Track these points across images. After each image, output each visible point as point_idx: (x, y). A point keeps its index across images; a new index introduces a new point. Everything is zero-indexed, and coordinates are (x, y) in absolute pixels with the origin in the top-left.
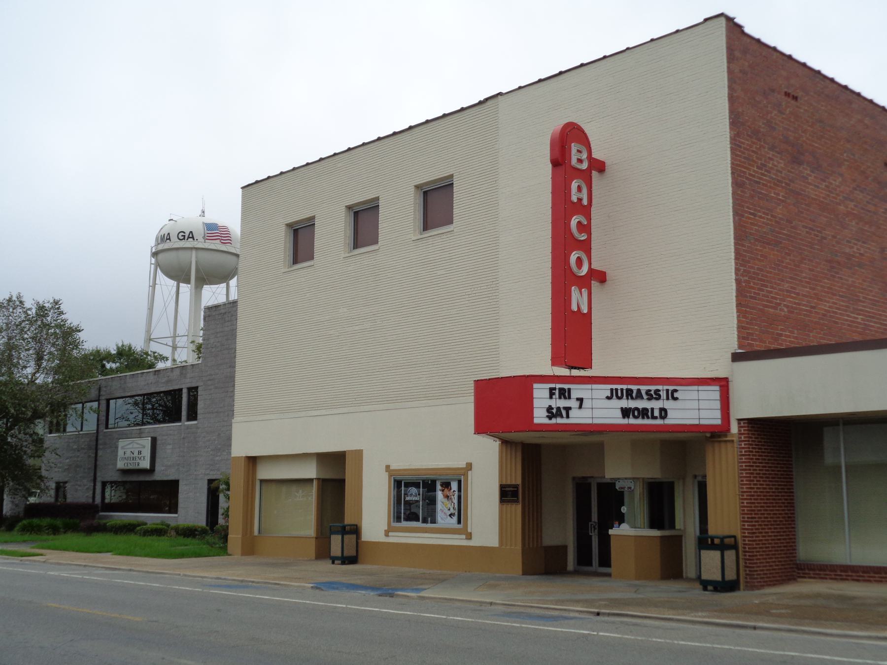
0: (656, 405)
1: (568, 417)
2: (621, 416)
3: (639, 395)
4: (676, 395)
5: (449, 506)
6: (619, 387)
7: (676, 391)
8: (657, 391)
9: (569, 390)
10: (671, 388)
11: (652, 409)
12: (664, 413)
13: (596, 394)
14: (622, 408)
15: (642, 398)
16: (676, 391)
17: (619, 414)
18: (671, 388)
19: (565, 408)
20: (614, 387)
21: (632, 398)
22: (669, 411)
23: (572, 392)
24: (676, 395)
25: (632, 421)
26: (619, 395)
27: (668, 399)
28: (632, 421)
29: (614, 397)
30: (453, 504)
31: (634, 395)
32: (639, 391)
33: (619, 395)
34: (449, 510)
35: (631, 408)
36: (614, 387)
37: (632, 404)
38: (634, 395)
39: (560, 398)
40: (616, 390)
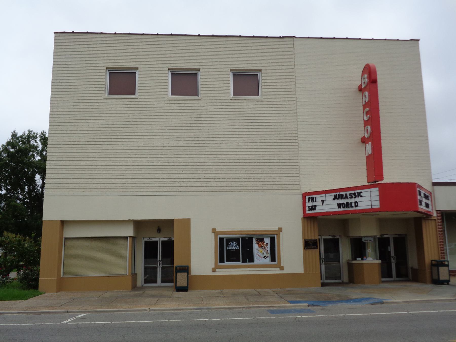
0: (353, 200)
1: (315, 210)
2: (337, 207)
3: (346, 197)
4: (361, 194)
5: (263, 252)
6: (338, 193)
7: (361, 192)
8: (354, 194)
9: (316, 197)
10: (359, 191)
11: (351, 203)
12: (356, 204)
13: (328, 198)
14: (337, 204)
15: (347, 198)
16: (361, 192)
17: (336, 206)
18: (359, 191)
19: (314, 206)
20: (336, 194)
21: (343, 199)
22: (358, 202)
23: (317, 198)
24: (361, 194)
25: (342, 209)
26: (338, 197)
27: (358, 197)
28: (342, 209)
29: (336, 199)
30: (266, 251)
31: (344, 197)
32: (346, 194)
33: (338, 197)
34: (264, 254)
35: (341, 203)
36: (336, 194)
37: (342, 201)
38: (344, 197)
39: (312, 202)
40: (337, 195)
